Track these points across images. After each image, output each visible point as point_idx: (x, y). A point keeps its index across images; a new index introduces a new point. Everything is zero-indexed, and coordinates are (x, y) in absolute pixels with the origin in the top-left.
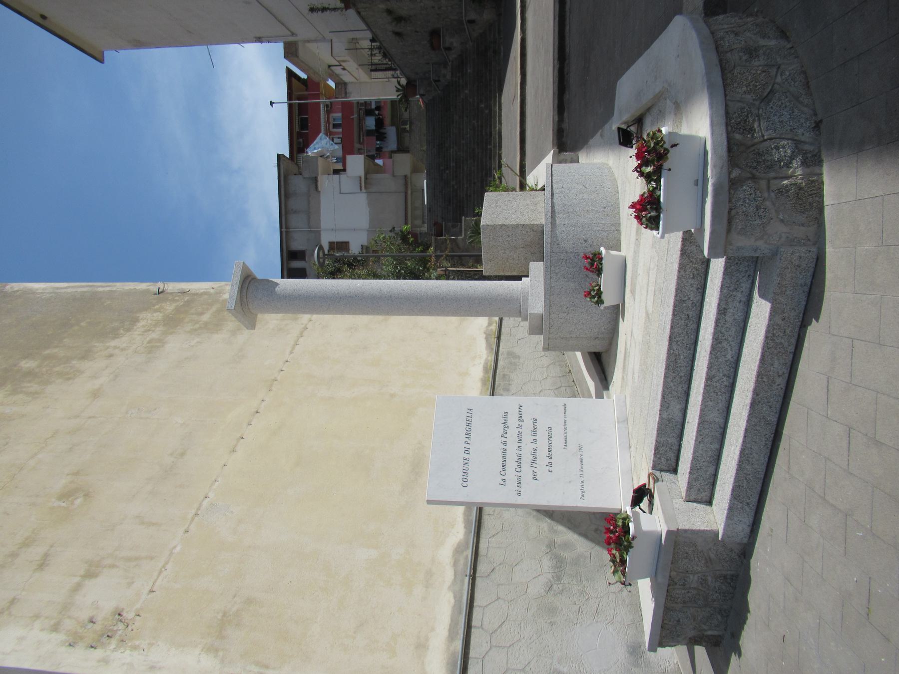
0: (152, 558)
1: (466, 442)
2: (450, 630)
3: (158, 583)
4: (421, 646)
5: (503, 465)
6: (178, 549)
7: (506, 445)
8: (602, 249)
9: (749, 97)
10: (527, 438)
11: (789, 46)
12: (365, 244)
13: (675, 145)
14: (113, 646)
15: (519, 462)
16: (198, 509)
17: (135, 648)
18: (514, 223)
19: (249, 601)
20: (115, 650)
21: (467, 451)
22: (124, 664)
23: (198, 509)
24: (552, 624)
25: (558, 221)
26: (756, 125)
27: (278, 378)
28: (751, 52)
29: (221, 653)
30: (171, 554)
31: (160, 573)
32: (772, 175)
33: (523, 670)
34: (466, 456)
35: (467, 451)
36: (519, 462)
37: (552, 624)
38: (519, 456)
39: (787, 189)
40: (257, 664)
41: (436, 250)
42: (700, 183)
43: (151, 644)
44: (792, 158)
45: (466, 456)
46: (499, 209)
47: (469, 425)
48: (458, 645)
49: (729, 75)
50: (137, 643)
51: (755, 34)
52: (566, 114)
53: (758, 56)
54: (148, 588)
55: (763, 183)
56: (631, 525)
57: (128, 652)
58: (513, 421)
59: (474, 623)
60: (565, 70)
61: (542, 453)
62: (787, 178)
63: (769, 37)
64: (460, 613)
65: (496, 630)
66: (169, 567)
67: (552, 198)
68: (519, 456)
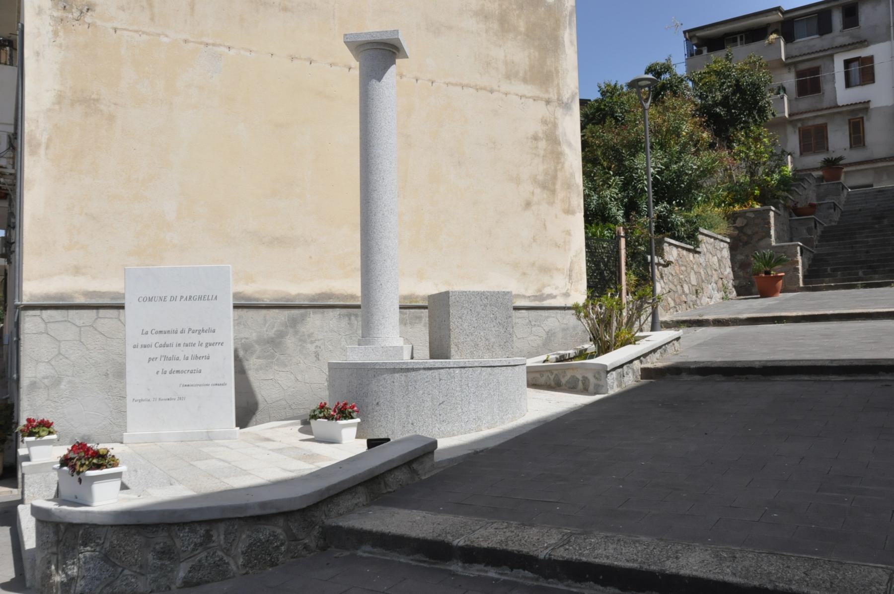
0: (152, 19)
1: (182, 297)
2: (95, 292)
3: (125, 32)
4: (77, 271)
5: (161, 332)
6: (165, 39)
7: (181, 332)
8: (358, 420)
9: (107, 545)
10: (189, 352)
11: (173, 587)
12: (872, 106)
13: (80, 480)
14: (55, 14)
15: (165, 345)
16: (214, 45)
17: (56, 33)
18: (452, 326)
19: (111, 118)
20: (52, 17)
21: (173, 299)
22: (39, 29)
23: (214, 45)
24: (107, 375)
25: (397, 375)
26: (89, 548)
27: (404, 79)
28: (167, 553)
29: (57, 107)
30: (159, 35)
31: (137, 31)
32: (60, 558)
33: (60, 353)
34: (168, 299)
35: (173, 299)
36: (165, 345)
37: (107, 375)
38: (171, 345)
39: (49, 568)
40: (50, 139)
41: (756, 212)
42: (75, 500)
43: (60, 46)
44: (66, 574)
45: (168, 299)
46: (479, 309)
47: (200, 298)
48: (81, 300)
49: (133, 531)
50: (61, 34)
51: (200, 561)
52: (697, 377)
53: (161, 559)
54: (119, 26)
55: (54, 550)
56: (32, 439)
57: (51, 28)
58: (206, 338)
59: (102, 312)
60: (750, 376)
61: (175, 365)
62: (57, 569)
63: (190, 572)
64: (112, 299)
65: (96, 330)
66: (144, 37)
67: (424, 369)
68: (171, 345)
